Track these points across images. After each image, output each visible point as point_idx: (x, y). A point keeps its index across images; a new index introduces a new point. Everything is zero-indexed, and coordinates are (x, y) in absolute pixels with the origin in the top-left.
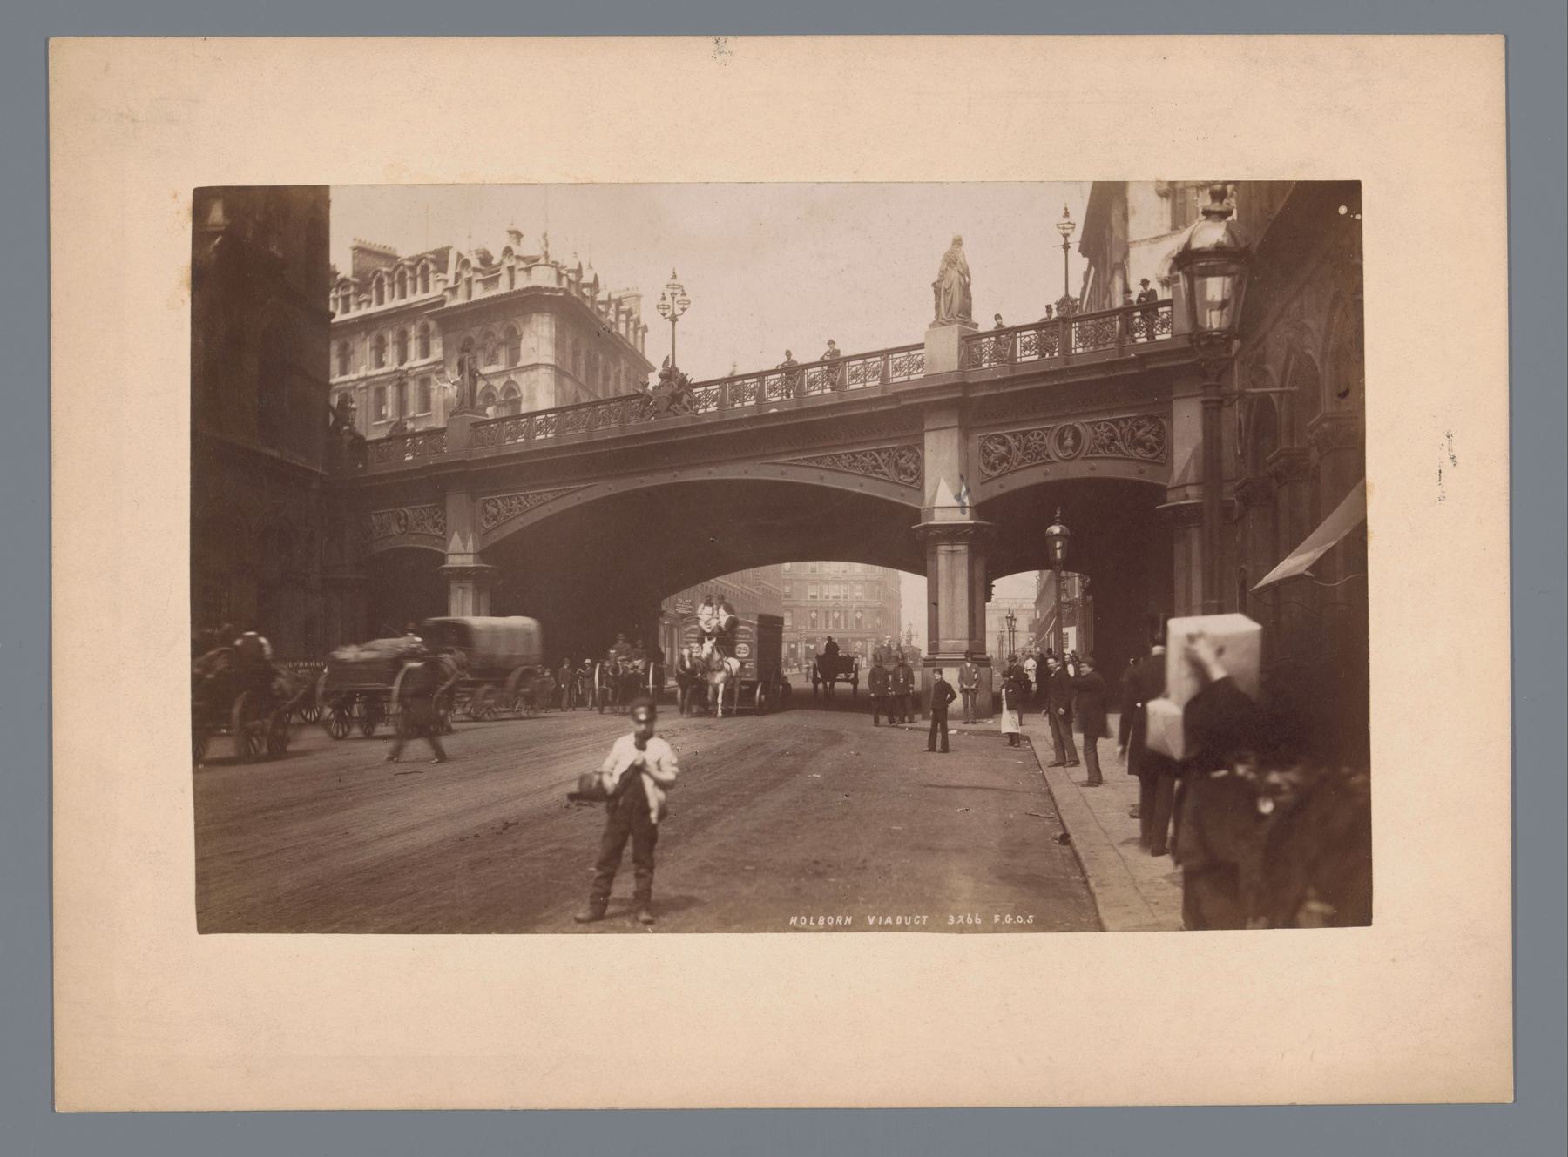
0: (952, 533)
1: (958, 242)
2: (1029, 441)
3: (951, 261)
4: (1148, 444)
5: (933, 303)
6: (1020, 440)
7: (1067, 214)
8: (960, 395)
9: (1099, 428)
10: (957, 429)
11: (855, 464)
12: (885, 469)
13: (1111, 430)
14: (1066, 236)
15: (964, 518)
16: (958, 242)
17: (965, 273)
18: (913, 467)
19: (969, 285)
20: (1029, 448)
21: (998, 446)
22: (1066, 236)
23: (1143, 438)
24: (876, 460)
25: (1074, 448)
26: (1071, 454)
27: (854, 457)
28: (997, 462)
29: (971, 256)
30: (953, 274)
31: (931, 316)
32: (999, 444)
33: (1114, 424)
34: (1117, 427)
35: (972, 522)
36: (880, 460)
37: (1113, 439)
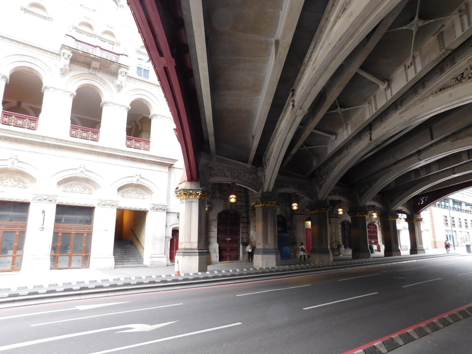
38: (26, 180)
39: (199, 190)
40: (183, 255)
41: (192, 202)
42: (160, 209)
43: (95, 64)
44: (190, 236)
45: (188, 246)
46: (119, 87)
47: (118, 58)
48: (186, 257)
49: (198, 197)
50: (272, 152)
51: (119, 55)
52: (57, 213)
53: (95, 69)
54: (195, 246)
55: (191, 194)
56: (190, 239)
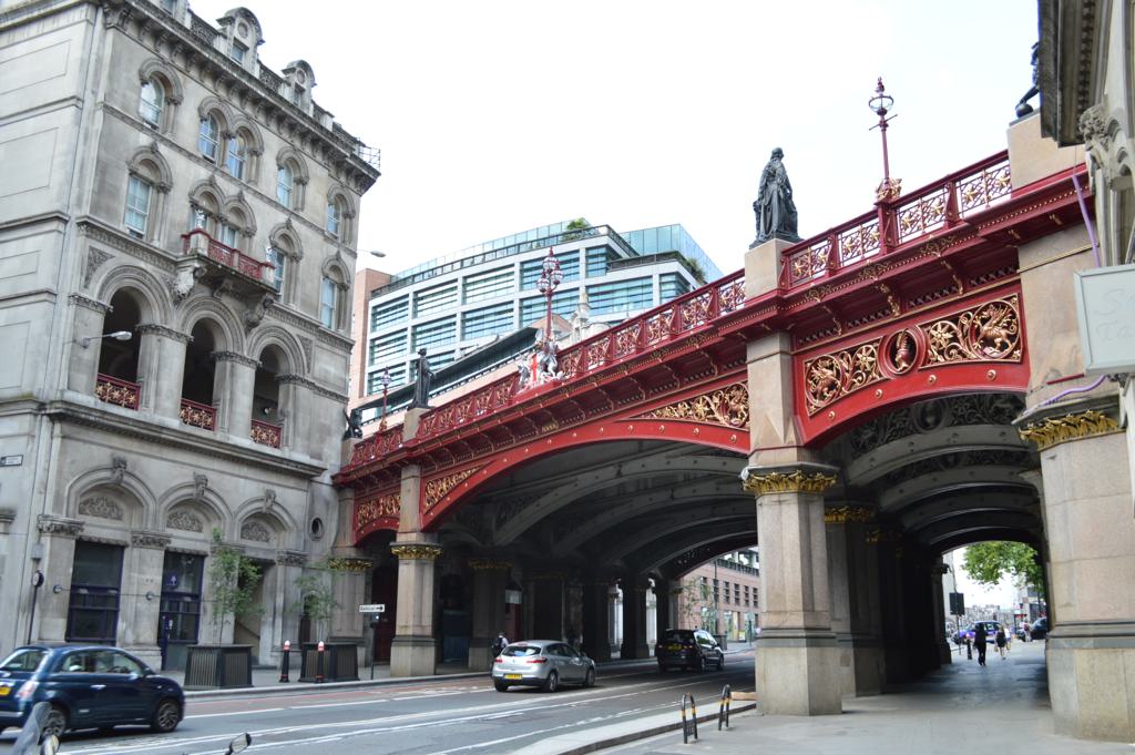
0: (781, 476)
1: (778, 154)
2: (858, 359)
3: (770, 175)
4: (998, 340)
5: (755, 222)
6: (848, 360)
7: (881, 88)
8: (775, 313)
9: (936, 329)
10: (779, 355)
11: (691, 413)
12: (717, 415)
13: (950, 329)
14: (882, 112)
15: (790, 457)
16: (778, 154)
17: (786, 185)
18: (742, 407)
19: (790, 197)
20: (858, 368)
21: (824, 370)
22: (882, 112)
23: (989, 334)
24: (709, 405)
25: (908, 359)
26: (905, 368)
27: (689, 405)
28: (826, 389)
29: (792, 167)
30: (773, 187)
31: (752, 235)
32: (827, 368)
33: (952, 321)
34: (956, 324)
35: (799, 463)
36: (713, 407)
37: (955, 339)
38: (122, 506)
39: (437, 547)
40: (414, 646)
41: (424, 564)
42: (296, 561)
43: (228, 283)
44: (421, 617)
45: (418, 632)
46: (251, 325)
47: (259, 275)
48: (417, 648)
49: (433, 557)
50: (539, 497)
51: (262, 265)
52: (77, 557)
53: (222, 291)
54: (428, 631)
55: (426, 552)
56: (421, 622)
